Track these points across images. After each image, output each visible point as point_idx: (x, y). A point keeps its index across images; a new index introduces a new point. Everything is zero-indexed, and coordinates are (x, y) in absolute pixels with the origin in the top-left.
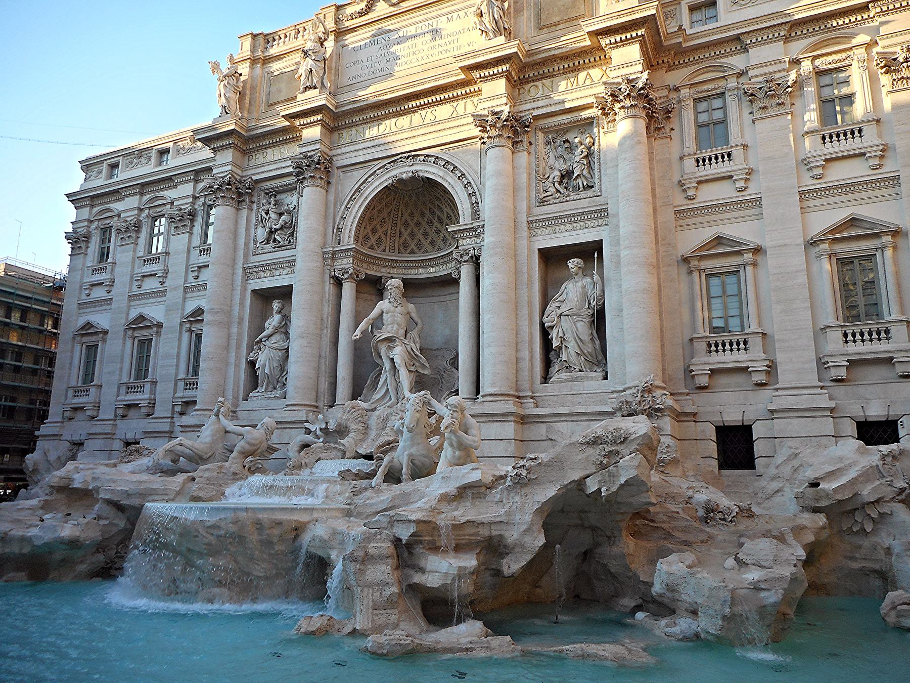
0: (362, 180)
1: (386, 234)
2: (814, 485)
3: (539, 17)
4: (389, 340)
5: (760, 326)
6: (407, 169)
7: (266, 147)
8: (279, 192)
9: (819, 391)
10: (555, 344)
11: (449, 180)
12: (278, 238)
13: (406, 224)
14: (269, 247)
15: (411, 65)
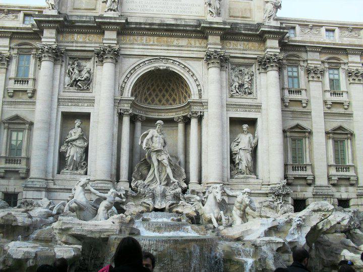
0: (136, 65)
1: (139, 92)
2: (339, 223)
3: (230, 12)
4: (158, 151)
5: (310, 162)
6: (163, 65)
7: (74, 33)
8: (80, 59)
9: (328, 188)
10: (237, 162)
11: (187, 76)
12: (80, 85)
13: (148, 89)
14: (72, 89)
15: (165, 13)
